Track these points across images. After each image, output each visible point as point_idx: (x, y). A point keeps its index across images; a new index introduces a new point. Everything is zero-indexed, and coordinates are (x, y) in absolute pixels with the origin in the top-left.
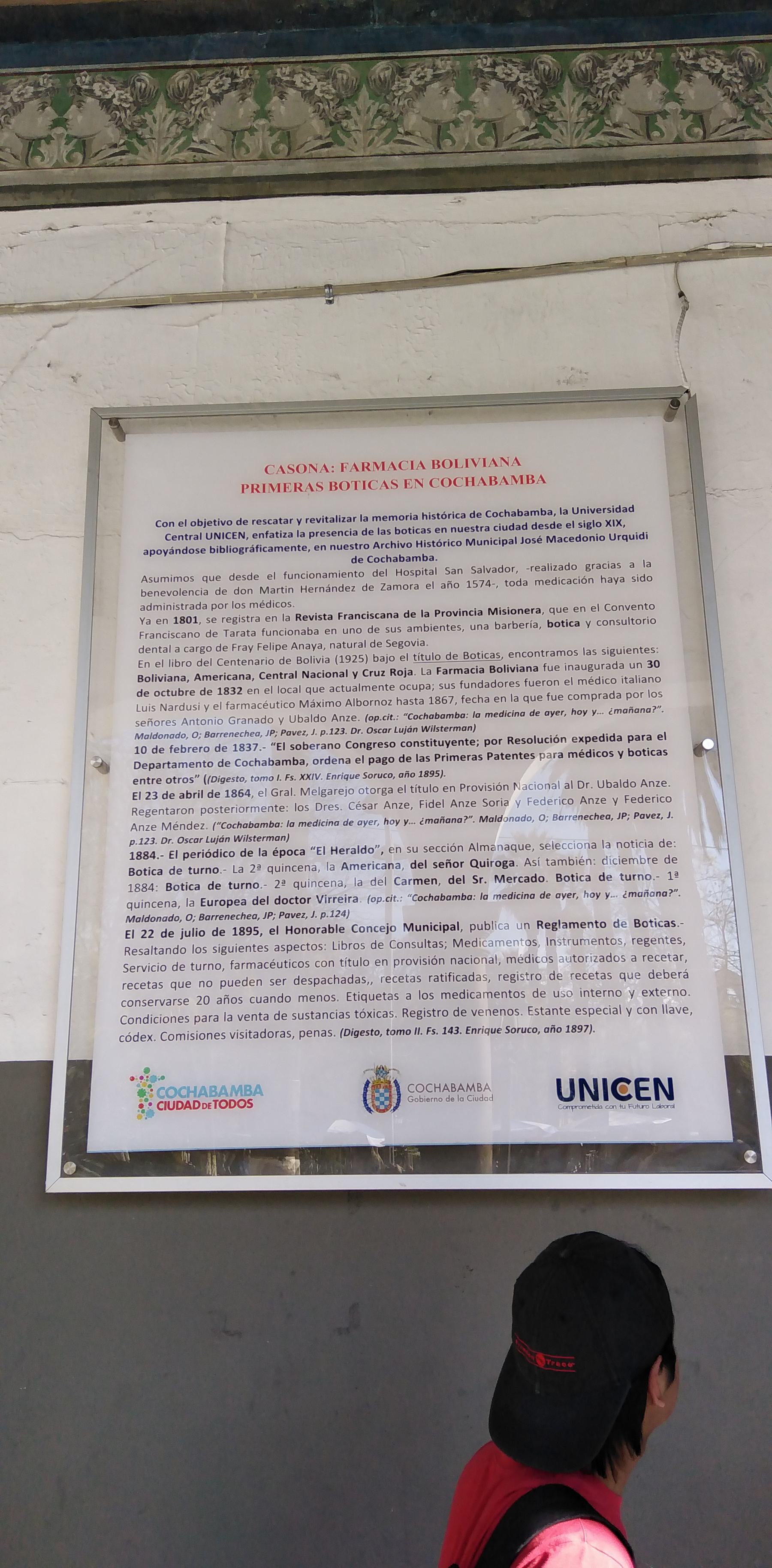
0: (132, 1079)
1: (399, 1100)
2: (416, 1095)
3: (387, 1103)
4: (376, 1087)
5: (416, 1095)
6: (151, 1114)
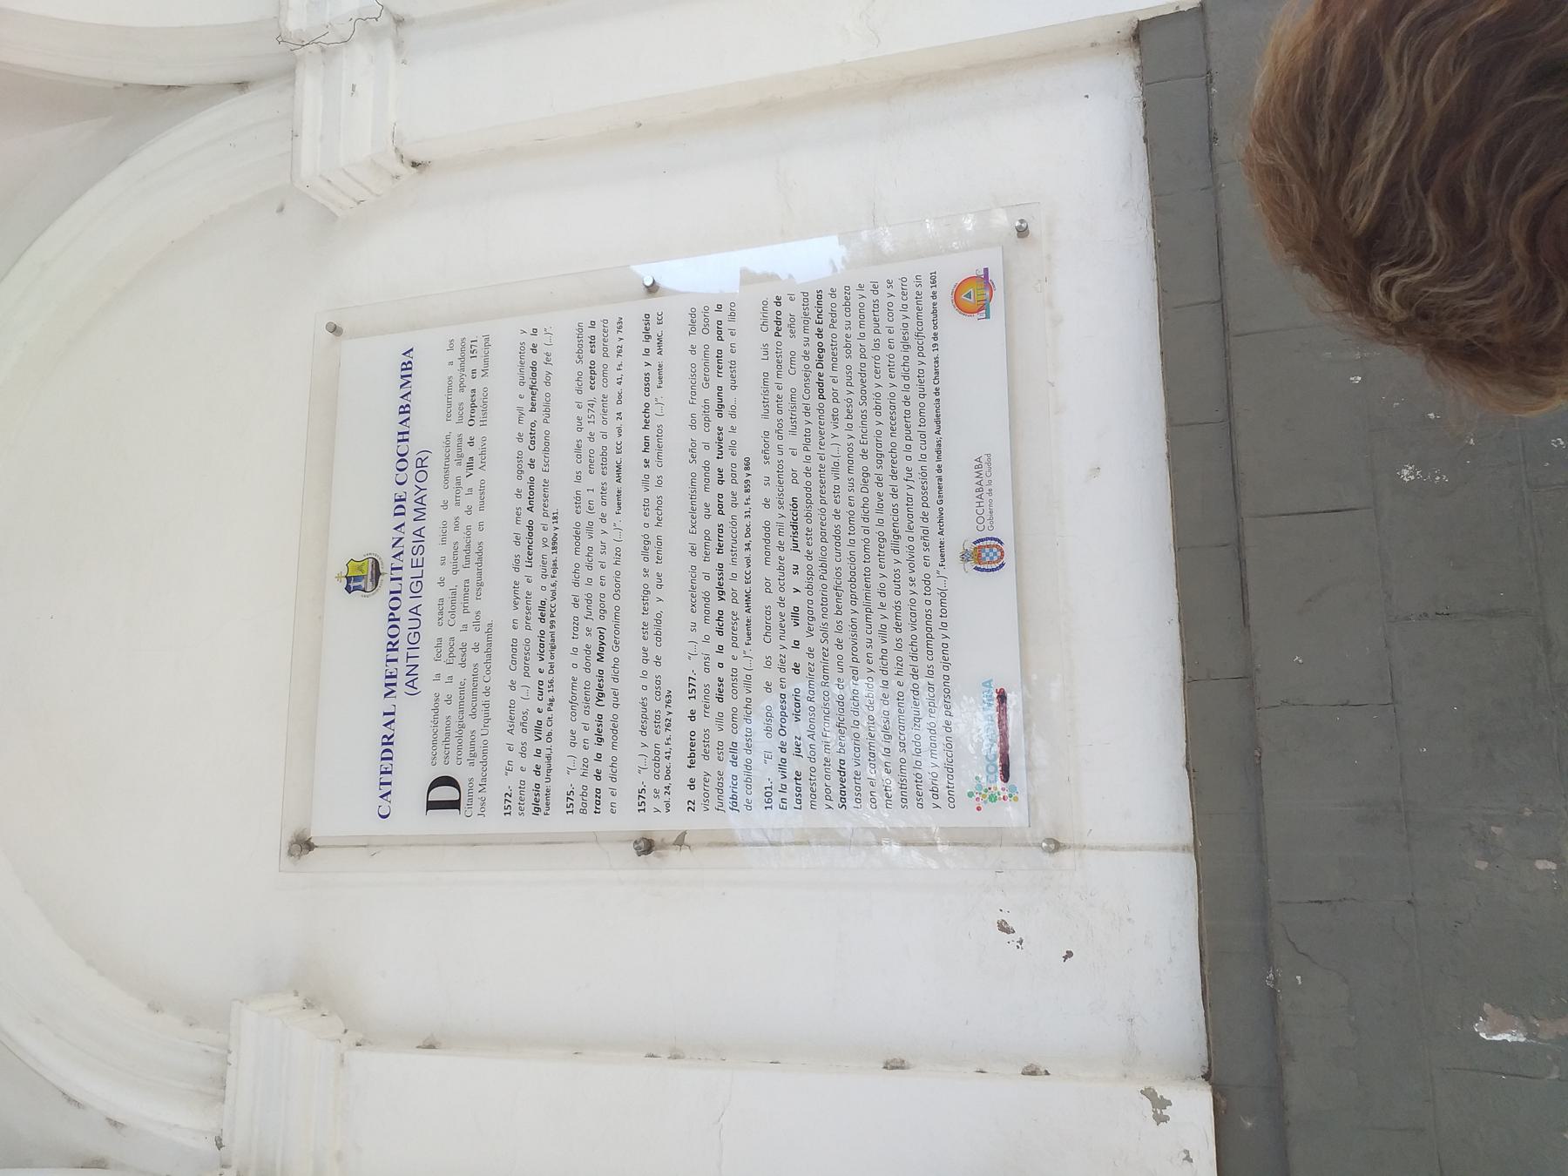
0: (979, 809)
1: (991, 539)
2: (987, 523)
3: (995, 550)
4: (979, 559)
5: (987, 523)
6: (1013, 788)
